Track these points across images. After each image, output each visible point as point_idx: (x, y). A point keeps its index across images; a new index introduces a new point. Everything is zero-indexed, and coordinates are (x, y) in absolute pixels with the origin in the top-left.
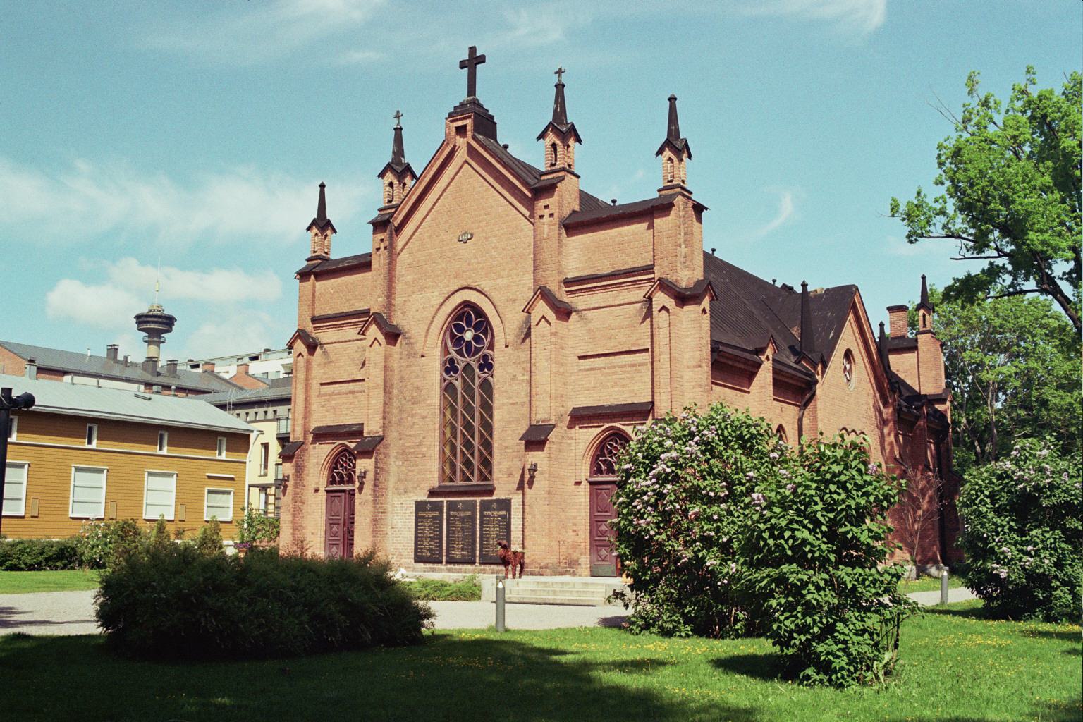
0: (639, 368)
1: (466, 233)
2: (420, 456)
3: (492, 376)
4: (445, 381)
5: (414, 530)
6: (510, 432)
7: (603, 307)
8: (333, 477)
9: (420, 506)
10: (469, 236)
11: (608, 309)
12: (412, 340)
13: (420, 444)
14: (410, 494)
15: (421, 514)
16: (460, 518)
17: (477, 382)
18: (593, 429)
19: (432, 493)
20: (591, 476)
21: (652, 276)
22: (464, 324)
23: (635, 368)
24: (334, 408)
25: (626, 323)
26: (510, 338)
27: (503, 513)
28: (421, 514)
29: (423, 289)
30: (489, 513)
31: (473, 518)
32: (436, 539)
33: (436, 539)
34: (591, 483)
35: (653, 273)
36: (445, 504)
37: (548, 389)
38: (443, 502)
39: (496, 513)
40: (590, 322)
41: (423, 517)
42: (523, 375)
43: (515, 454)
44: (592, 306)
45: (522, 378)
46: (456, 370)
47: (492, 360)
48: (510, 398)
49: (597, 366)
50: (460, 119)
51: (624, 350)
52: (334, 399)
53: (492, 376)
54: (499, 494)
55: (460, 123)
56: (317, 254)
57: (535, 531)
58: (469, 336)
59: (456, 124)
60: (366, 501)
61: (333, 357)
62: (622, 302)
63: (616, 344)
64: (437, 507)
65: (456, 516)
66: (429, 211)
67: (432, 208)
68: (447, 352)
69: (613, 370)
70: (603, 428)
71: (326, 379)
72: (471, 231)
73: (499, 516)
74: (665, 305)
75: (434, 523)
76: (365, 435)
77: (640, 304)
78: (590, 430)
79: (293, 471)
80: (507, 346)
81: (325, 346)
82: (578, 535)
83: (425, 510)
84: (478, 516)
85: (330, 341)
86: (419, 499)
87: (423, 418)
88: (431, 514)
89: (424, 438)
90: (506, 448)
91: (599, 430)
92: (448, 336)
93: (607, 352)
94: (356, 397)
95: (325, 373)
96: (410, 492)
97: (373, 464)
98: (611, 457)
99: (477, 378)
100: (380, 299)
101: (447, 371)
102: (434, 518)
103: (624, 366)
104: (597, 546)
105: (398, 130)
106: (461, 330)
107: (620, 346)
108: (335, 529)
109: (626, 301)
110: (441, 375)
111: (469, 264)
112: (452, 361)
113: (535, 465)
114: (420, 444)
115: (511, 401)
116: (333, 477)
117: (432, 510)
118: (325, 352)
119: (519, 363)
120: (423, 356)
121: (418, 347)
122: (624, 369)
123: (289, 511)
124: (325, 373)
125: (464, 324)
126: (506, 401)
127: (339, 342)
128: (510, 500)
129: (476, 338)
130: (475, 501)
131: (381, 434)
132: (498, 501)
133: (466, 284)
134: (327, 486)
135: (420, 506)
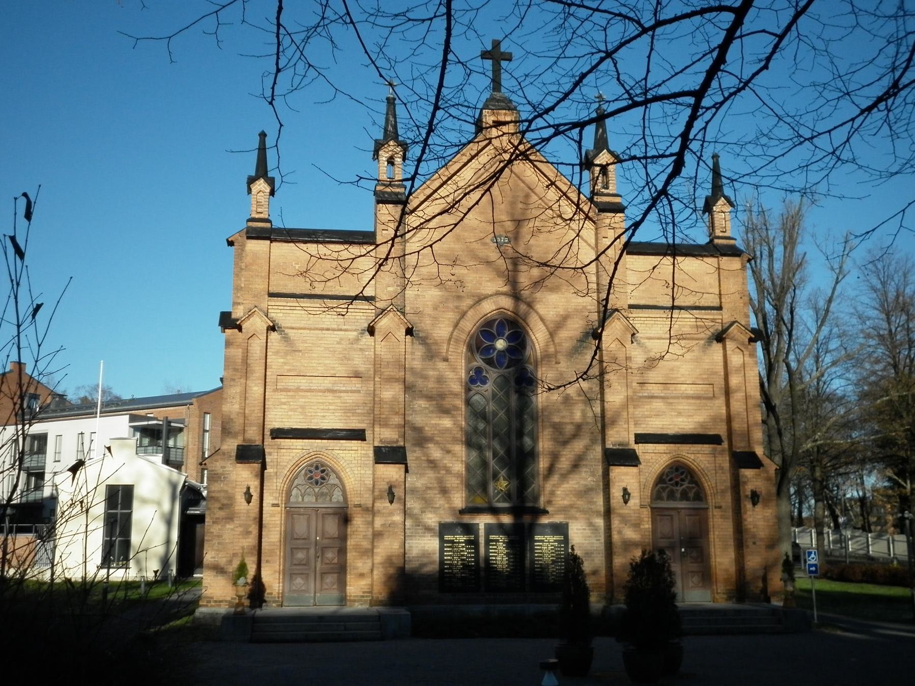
24: (303, 407)
27: (562, 538)
34: (652, 508)
44: (652, 335)
52: (303, 397)
61: (301, 346)
71: (289, 370)
73: (555, 541)
75: (467, 549)
85: (293, 325)
95: (285, 363)
98: (682, 485)
106: (492, 338)
108: (300, 555)
118: (286, 338)
124: (285, 363)
127: (310, 329)
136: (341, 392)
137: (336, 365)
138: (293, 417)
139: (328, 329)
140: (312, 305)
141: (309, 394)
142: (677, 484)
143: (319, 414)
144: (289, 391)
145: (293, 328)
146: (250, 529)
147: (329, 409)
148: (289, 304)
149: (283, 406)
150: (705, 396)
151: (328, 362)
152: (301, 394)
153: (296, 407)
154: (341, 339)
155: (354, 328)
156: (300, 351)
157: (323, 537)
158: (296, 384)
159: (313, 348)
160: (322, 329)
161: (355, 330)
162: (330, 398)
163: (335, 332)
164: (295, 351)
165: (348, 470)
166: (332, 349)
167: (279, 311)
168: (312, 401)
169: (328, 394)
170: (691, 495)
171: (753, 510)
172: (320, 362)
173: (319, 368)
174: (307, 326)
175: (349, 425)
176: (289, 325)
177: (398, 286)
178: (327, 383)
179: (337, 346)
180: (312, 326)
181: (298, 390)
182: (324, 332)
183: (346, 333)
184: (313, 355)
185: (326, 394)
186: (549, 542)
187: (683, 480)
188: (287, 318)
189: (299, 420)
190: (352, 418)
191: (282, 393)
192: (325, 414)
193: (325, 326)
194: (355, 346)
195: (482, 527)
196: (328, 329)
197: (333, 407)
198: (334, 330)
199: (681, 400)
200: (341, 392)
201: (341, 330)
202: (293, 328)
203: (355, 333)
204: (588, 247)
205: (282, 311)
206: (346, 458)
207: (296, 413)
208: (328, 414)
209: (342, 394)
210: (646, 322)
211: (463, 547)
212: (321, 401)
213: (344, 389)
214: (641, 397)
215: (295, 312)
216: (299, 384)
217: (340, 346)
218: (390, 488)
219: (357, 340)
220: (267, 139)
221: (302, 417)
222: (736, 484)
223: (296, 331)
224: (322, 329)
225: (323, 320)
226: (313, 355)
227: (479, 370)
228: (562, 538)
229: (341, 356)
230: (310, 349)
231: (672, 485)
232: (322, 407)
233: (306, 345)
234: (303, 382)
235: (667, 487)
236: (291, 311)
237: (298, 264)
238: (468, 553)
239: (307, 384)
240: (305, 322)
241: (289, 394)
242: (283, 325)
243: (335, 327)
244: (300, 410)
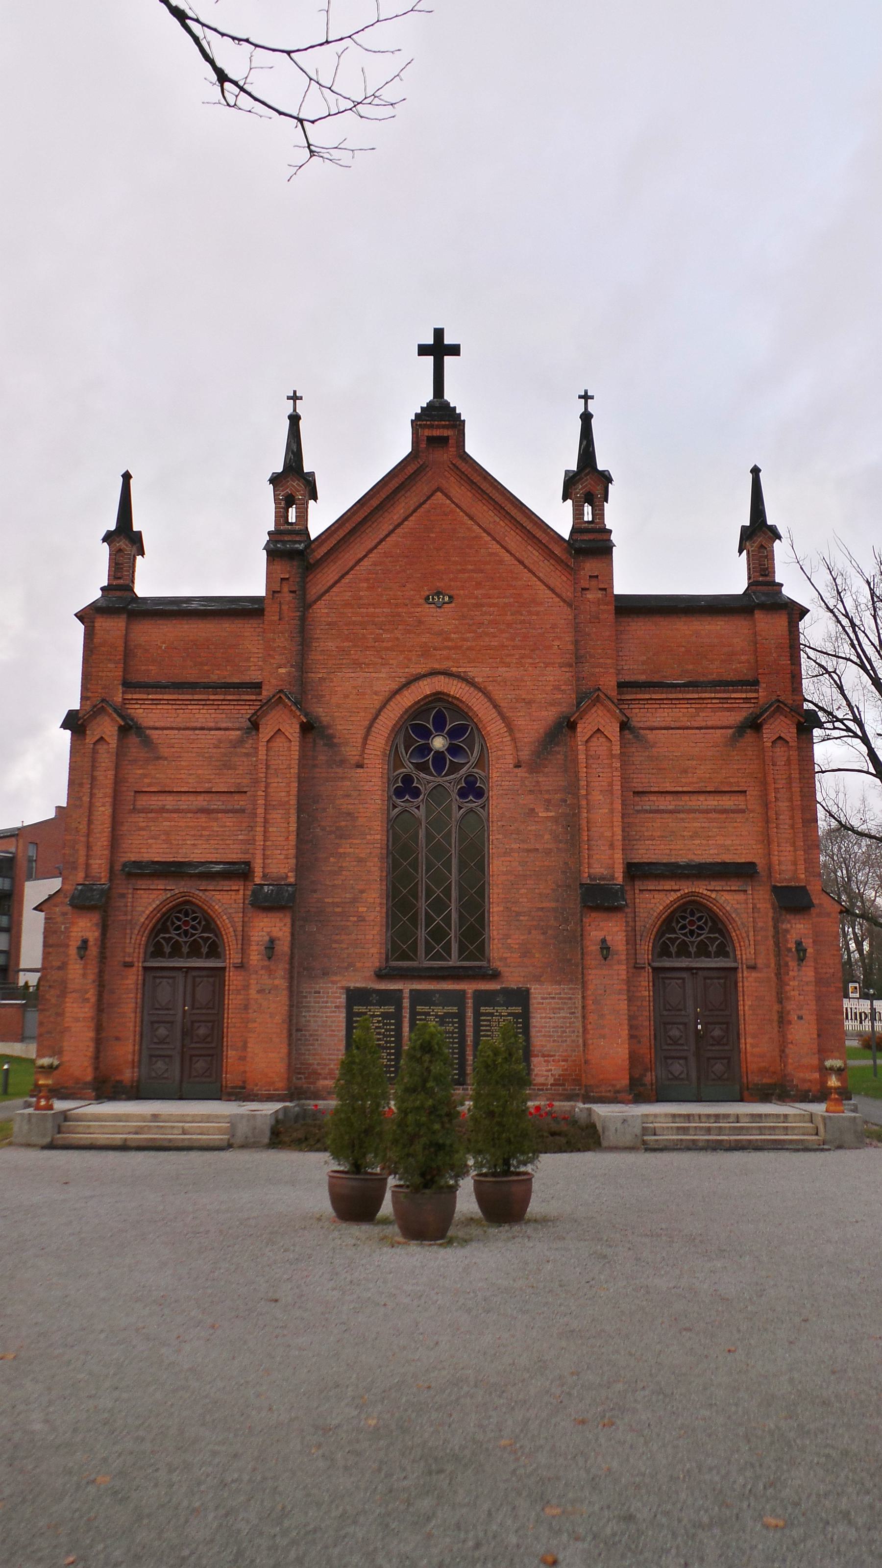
0: (732, 815)
1: (438, 594)
2: (355, 919)
3: (483, 807)
4: (395, 807)
5: (344, 1033)
6: (523, 891)
7: (672, 729)
8: (158, 945)
9: (356, 997)
10: (447, 599)
11: (681, 731)
12: (335, 741)
13: (355, 900)
14: (335, 978)
15: (356, 1009)
16: (437, 1016)
17: (457, 814)
18: (661, 895)
19: (380, 976)
20: (653, 961)
21: (754, 695)
22: (431, 727)
23: (724, 816)
24: (167, 833)
25: (710, 753)
26: (525, 754)
27: (518, 1010)
28: (356, 1009)
29: (357, 665)
30: (490, 1010)
31: (461, 1016)
32: (390, 1048)
33: (390, 1048)
34: (654, 969)
35: (757, 691)
36: (406, 994)
37: (609, 834)
38: (401, 991)
39: (504, 1011)
40: (652, 747)
41: (360, 1014)
42: (547, 810)
43: (535, 923)
44: (656, 724)
45: (544, 814)
46: (416, 793)
47: (483, 782)
48: (523, 841)
49: (661, 807)
50: (438, 427)
51: (708, 789)
53: (483, 807)
54: (513, 979)
55: (436, 433)
56: (121, 582)
57: (603, 1037)
58: (439, 743)
59: (427, 433)
60: (276, 987)
61: (164, 751)
62: (703, 724)
63: (695, 780)
64: (394, 998)
65: (492, 1015)
66: (371, 551)
67: (375, 547)
68: (398, 763)
69: (692, 816)
70: (679, 894)
71: (149, 785)
72: (451, 593)
73: (510, 1014)
74: (782, 735)
76: (258, 881)
77: (730, 731)
78: (657, 895)
79: (97, 934)
80: (518, 766)
81: (148, 732)
82: (639, 1042)
83: (367, 1003)
84: (406, 1014)
85: (157, 724)
86: (352, 985)
87: (360, 860)
88: (378, 1011)
89: (362, 892)
90: (518, 914)
91: (673, 896)
92: (400, 740)
93: (680, 789)
94: (216, 819)
96: (336, 974)
97: (287, 929)
99: (455, 807)
100: (282, 671)
101: (399, 793)
102: (385, 1015)
103: (707, 811)
104: (666, 1058)
105: (294, 419)
106: (426, 734)
107: (703, 784)
108: (162, 1031)
109: (710, 723)
110: (390, 798)
111: (448, 639)
112: (407, 779)
113: (604, 941)
114: (355, 900)
115: (522, 846)
116: (158, 945)
117: (381, 1004)
119: (541, 793)
120: (360, 766)
121: (351, 752)
122: (710, 815)
123: (87, 1000)
125: (431, 727)
126: (515, 846)
127: (179, 729)
128: (528, 990)
129: (453, 750)
130: (464, 992)
131: (292, 880)
132: (506, 992)
133: (437, 666)
134: (144, 961)
135: (356, 997)
136: (218, 811)
137: (212, 777)
138: (154, 846)
139: (202, 729)
140: (181, 697)
141: (175, 815)
142: (692, 933)
143: (188, 842)
144: (152, 811)
145: (156, 729)
146: (87, 996)
147: (201, 836)
148: (150, 697)
149: (142, 833)
150: (733, 807)
151: (200, 772)
152: (164, 815)
153: (158, 833)
154: (220, 741)
155: (237, 725)
156: (166, 759)
157: (193, 1007)
158: (160, 803)
159: (182, 754)
160: (195, 729)
161: (238, 729)
162: (204, 820)
163: (212, 732)
164: (159, 758)
165: (225, 917)
166: (206, 755)
167: (138, 706)
168: (180, 824)
169: (203, 815)
170: (713, 949)
171: (799, 970)
172: (191, 772)
173: (190, 781)
174: (174, 725)
175: (230, 856)
176: (151, 724)
177: (292, 666)
178: (200, 801)
179: (215, 750)
180: (182, 725)
181: (163, 810)
182: (197, 732)
183: (227, 732)
184: (183, 763)
185: (199, 815)
186: (501, 1016)
187: (700, 928)
188: (150, 715)
189: (161, 851)
190: (232, 847)
191: (141, 815)
192: (196, 842)
193: (199, 725)
194: (238, 750)
195: (406, 994)
196: (202, 729)
197: (207, 833)
198: (210, 729)
199: (697, 815)
200: (218, 811)
201: (219, 729)
202: (156, 729)
203: (238, 733)
204: (562, 604)
205: (143, 707)
206: (224, 901)
207: (159, 841)
208: (200, 842)
209: (220, 815)
210: (646, 706)
211: (379, 1022)
212: (190, 824)
213: (224, 807)
214: (638, 811)
215: (159, 707)
216: (164, 803)
217: (219, 750)
218: (272, 941)
219: (241, 742)
220: (132, 481)
221: (165, 846)
222: (778, 936)
223: (157, 732)
224: (195, 729)
225: (197, 716)
226: (183, 763)
227: (407, 779)
228: (518, 1010)
229: (219, 763)
230: (176, 755)
231: (685, 935)
232: (192, 833)
233: (173, 750)
234: (169, 802)
235: (678, 938)
236: (154, 707)
237: (164, 643)
238: (387, 1030)
239: (174, 803)
240: (172, 719)
241: (150, 815)
242: (145, 725)
243: (212, 725)
244: (163, 837)
